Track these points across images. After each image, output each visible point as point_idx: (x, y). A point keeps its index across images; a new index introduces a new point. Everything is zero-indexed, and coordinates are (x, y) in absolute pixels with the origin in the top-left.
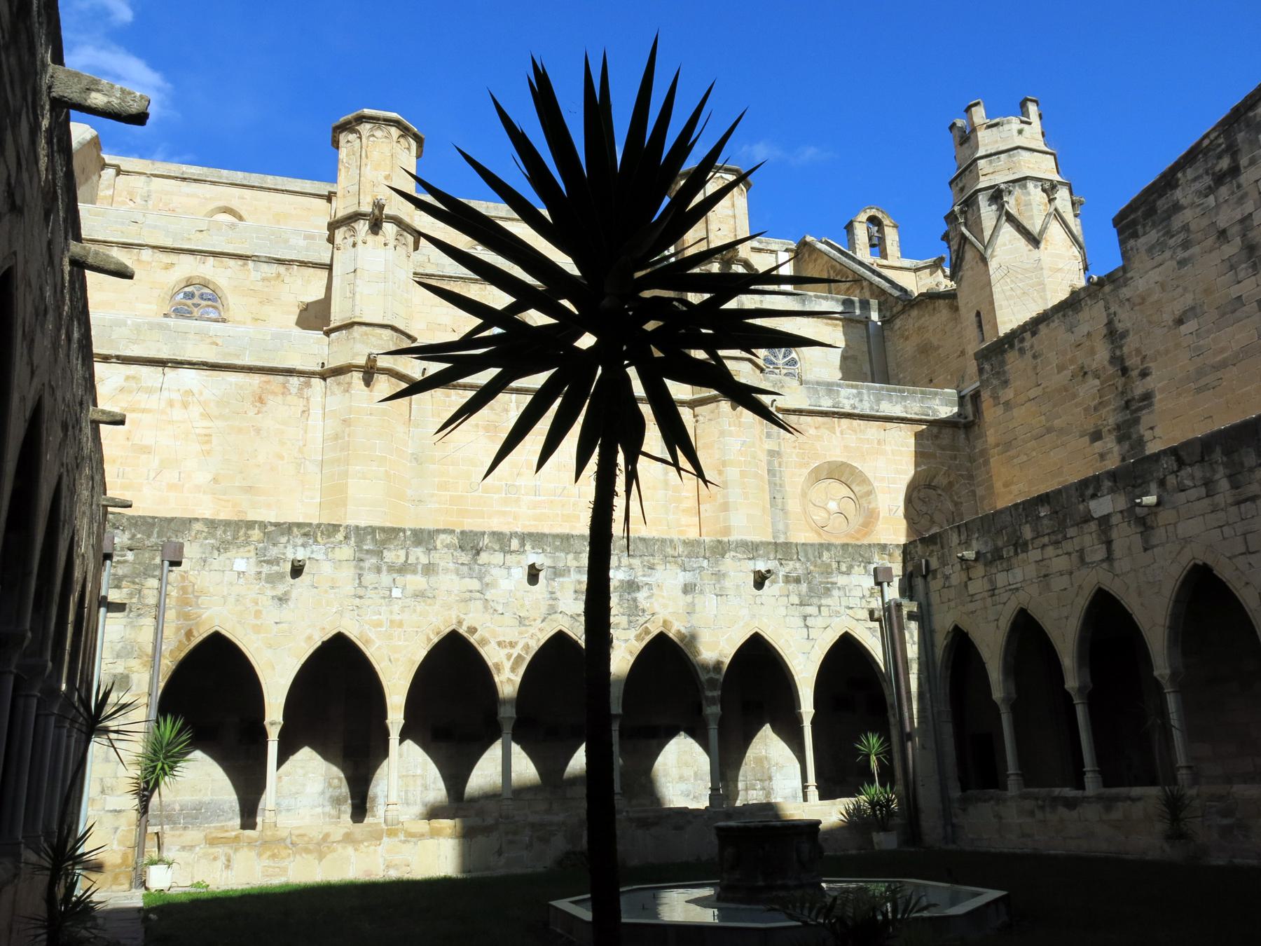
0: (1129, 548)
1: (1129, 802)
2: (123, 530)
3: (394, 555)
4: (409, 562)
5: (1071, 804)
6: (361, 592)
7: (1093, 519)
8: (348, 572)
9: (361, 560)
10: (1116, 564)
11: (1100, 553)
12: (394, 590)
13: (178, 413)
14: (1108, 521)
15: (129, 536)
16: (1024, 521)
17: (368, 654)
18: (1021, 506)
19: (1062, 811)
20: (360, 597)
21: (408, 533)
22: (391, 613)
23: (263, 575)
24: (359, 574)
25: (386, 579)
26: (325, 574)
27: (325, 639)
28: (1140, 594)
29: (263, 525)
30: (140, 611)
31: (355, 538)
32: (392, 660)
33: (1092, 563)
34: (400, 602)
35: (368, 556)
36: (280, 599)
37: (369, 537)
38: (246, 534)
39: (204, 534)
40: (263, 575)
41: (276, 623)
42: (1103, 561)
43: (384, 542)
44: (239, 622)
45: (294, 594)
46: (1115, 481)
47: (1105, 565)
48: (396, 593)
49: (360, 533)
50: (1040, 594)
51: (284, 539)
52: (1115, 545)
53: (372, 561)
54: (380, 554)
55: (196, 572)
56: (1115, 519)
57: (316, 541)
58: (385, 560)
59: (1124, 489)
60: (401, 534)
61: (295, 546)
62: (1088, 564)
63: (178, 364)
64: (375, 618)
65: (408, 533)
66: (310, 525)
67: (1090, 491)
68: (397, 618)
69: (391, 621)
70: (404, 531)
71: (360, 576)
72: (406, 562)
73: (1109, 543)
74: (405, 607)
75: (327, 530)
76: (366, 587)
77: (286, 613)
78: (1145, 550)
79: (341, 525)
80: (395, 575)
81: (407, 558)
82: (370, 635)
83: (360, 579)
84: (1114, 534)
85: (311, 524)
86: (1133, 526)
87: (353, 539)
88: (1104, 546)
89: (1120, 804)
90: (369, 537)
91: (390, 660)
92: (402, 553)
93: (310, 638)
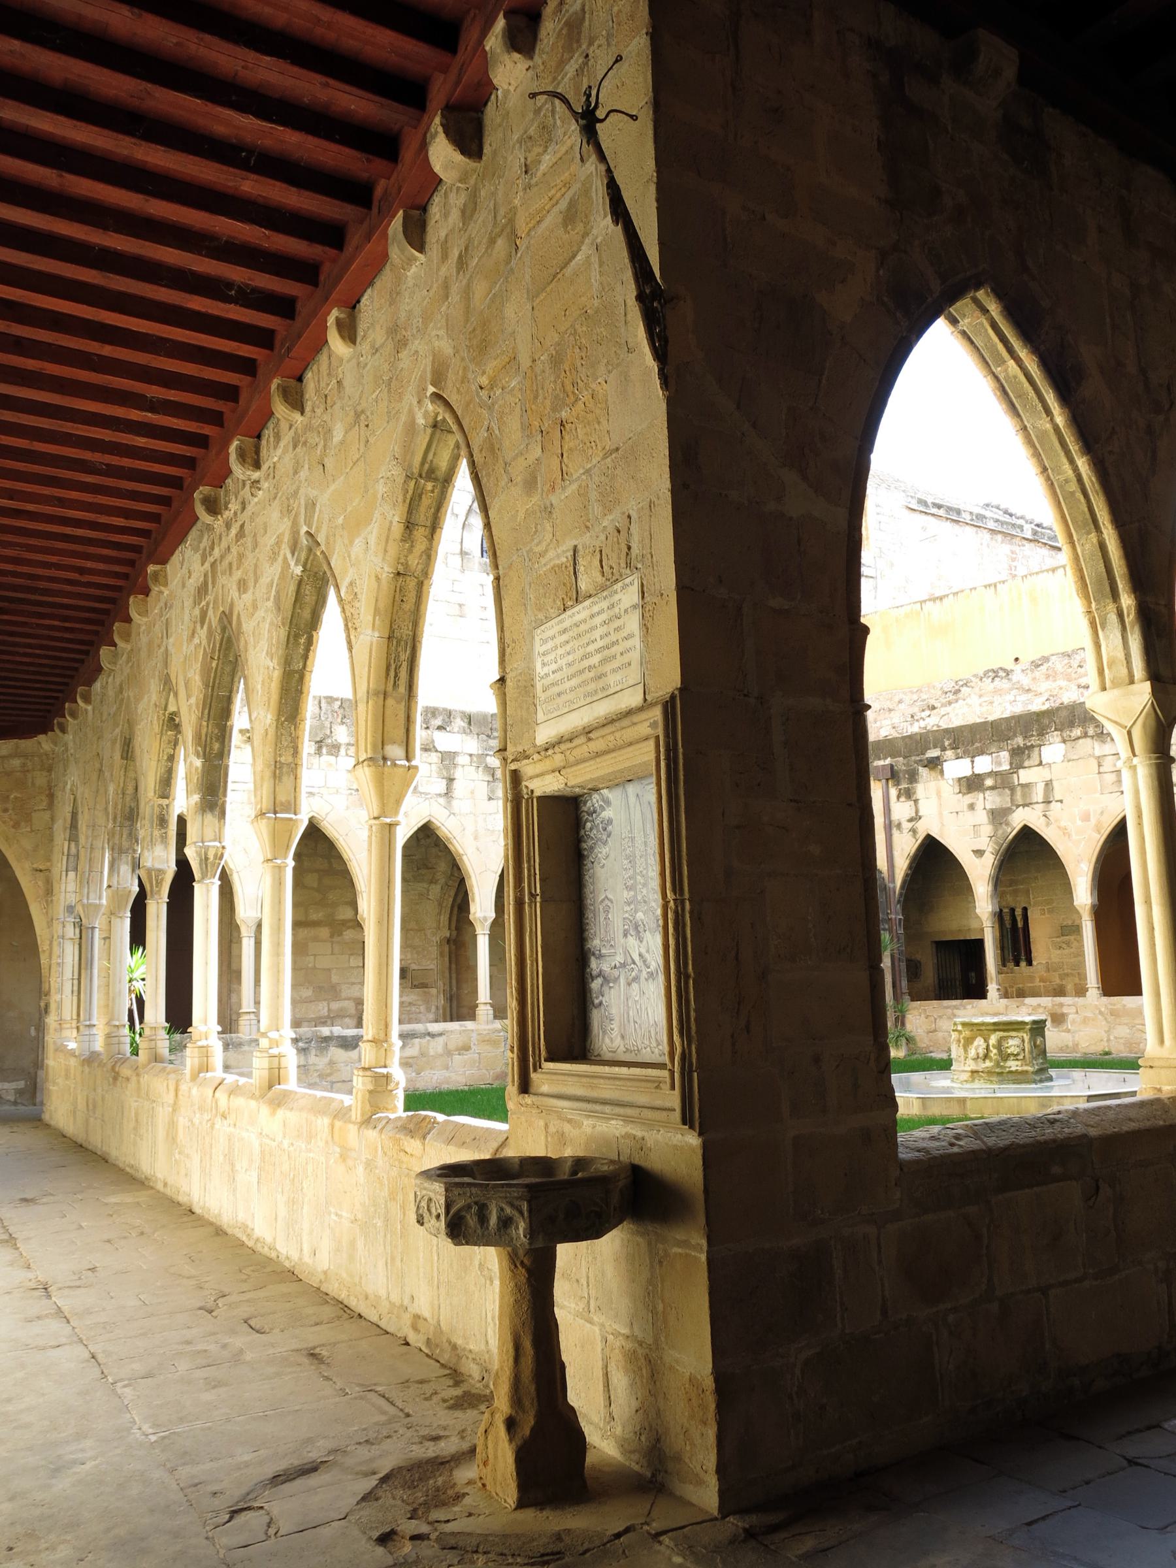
0: (472, 793)
1: (428, 1038)
5: (349, 1044)
7: (437, 751)
10: (455, 803)
11: (441, 786)
14: (454, 758)
16: (339, 720)
18: (339, 703)
19: (336, 1053)
28: (476, 838)
33: (427, 794)
42: (440, 795)
46: (470, 723)
47: (442, 800)
50: (348, 808)
52: (456, 785)
56: (462, 760)
59: (478, 734)
62: (421, 793)
67: (438, 722)
73: (451, 780)
78: (490, 799)
84: (458, 774)
86: (480, 773)
88: (444, 782)
89: (417, 1040)
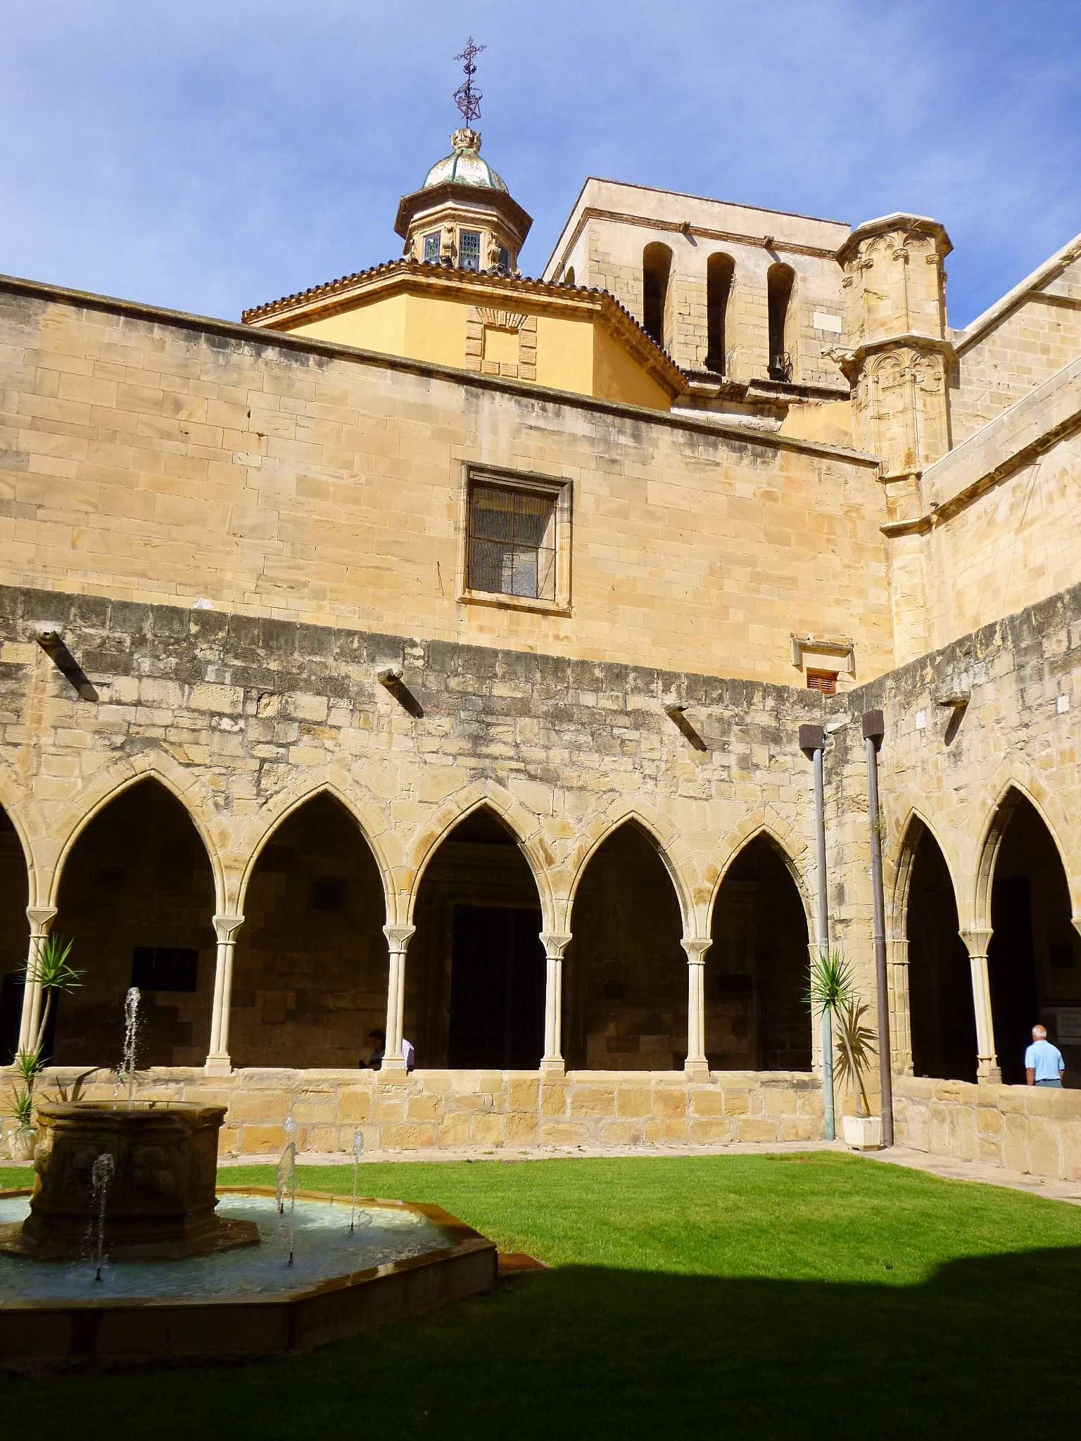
2: (845, 712)
3: (1055, 645)
4: (1073, 647)
6: (1026, 717)
8: (1010, 688)
9: (1022, 666)
12: (1060, 699)
13: (1059, 508)
15: (851, 717)
17: (1041, 812)
20: (1026, 726)
21: (1067, 598)
22: (1060, 738)
23: (939, 726)
24: (1022, 690)
25: (1049, 685)
26: (989, 703)
27: (999, 801)
29: (931, 657)
30: (844, 807)
31: (1012, 634)
32: (1068, 816)
34: (1067, 717)
35: (1027, 659)
36: (955, 756)
37: (1025, 627)
38: (921, 675)
39: (894, 691)
40: (939, 726)
41: (956, 789)
43: (1039, 631)
44: (927, 798)
45: (965, 745)
48: (1063, 705)
49: (1014, 625)
51: (950, 670)
53: (1033, 661)
54: (1038, 648)
55: (893, 742)
57: (977, 658)
58: (1046, 655)
60: (1059, 605)
61: (960, 674)
63: (1044, 444)
64: (1043, 753)
65: (1067, 598)
66: (968, 637)
68: (1066, 745)
69: (1062, 753)
70: (1059, 597)
71: (1022, 691)
72: (1069, 648)
74: (1074, 724)
75: (985, 636)
76: (1029, 708)
77: (963, 776)
79: (995, 624)
80: (1059, 675)
81: (1070, 642)
82: (1041, 783)
83: (1022, 697)
85: (970, 635)
87: (1010, 638)
90: (1025, 627)
91: (1065, 818)
92: (1063, 635)
93: (984, 803)
